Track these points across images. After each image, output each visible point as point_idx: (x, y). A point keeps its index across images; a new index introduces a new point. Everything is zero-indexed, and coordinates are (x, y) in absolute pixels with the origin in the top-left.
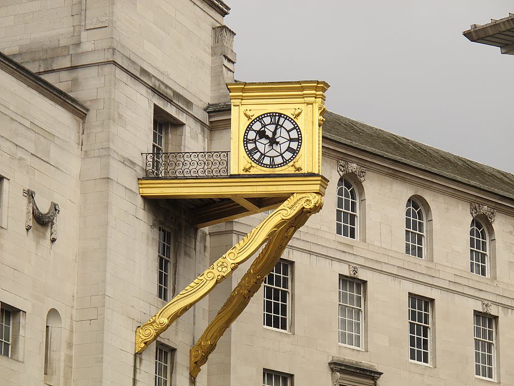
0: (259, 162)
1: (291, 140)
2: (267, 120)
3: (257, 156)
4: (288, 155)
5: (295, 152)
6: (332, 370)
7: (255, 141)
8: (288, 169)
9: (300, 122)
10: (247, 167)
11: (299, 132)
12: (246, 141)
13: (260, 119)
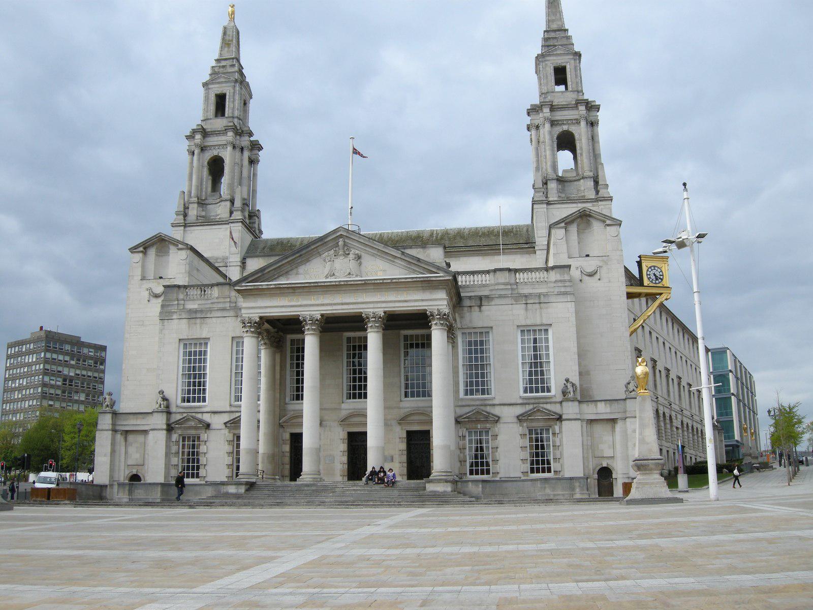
0: (652, 282)
1: (660, 275)
2: (653, 268)
3: (651, 280)
4: (660, 280)
5: (662, 280)
6: (635, 350)
7: (650, 275)
8: (660, 285)
9: (663, 269)
10: (648, 283)
11: (662, 272)
12: (647, 275)
13: (650, 267)
